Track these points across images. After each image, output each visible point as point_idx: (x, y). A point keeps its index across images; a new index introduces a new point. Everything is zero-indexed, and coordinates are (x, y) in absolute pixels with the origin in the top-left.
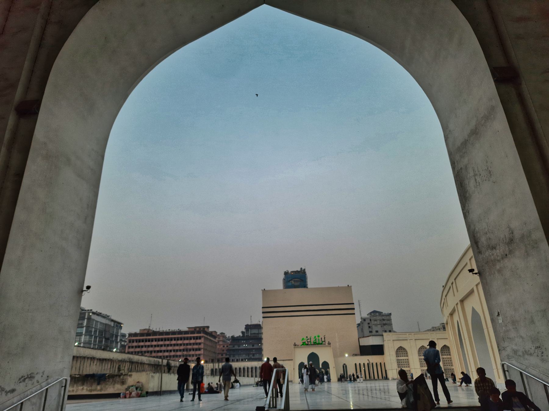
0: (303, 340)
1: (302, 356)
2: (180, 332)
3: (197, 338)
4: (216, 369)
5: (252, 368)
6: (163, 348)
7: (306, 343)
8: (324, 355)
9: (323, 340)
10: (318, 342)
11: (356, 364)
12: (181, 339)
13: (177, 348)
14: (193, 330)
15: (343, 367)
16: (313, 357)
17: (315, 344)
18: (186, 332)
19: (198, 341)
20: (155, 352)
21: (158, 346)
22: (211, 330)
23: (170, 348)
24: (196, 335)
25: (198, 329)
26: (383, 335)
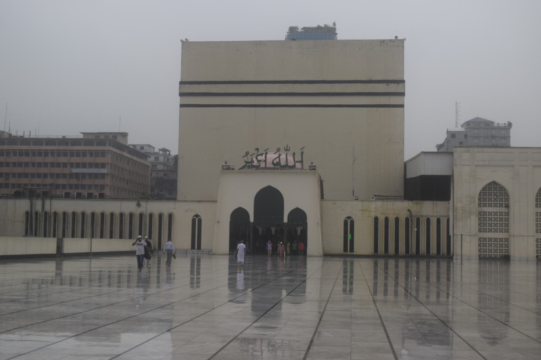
0: (247, 154)
1: (241, 194)
2: (64, 141)
3: (97, 154)
4: (37, 213)
5: (121, 215)
6: (31, 170)
7: (255, 163)
8: (297, 194)
9: (298, 158)
10: (283, 163)
11: (376, 219)
12: (65, 154)
13: (57, 170)
14: (93, 137)
15: (346, 223)
16: (269, 199)
17: (278, 166)
18: (75, 142)
19: (100, 160)
20: (14, 175)
21: (20, 165)
22: (131, 141)
23: (43, 170)
24: (95, 148)
25: (102, 137)
26: (452, 153)
